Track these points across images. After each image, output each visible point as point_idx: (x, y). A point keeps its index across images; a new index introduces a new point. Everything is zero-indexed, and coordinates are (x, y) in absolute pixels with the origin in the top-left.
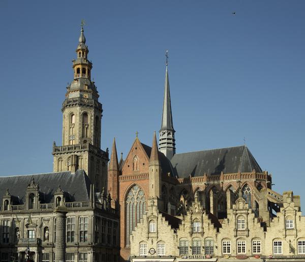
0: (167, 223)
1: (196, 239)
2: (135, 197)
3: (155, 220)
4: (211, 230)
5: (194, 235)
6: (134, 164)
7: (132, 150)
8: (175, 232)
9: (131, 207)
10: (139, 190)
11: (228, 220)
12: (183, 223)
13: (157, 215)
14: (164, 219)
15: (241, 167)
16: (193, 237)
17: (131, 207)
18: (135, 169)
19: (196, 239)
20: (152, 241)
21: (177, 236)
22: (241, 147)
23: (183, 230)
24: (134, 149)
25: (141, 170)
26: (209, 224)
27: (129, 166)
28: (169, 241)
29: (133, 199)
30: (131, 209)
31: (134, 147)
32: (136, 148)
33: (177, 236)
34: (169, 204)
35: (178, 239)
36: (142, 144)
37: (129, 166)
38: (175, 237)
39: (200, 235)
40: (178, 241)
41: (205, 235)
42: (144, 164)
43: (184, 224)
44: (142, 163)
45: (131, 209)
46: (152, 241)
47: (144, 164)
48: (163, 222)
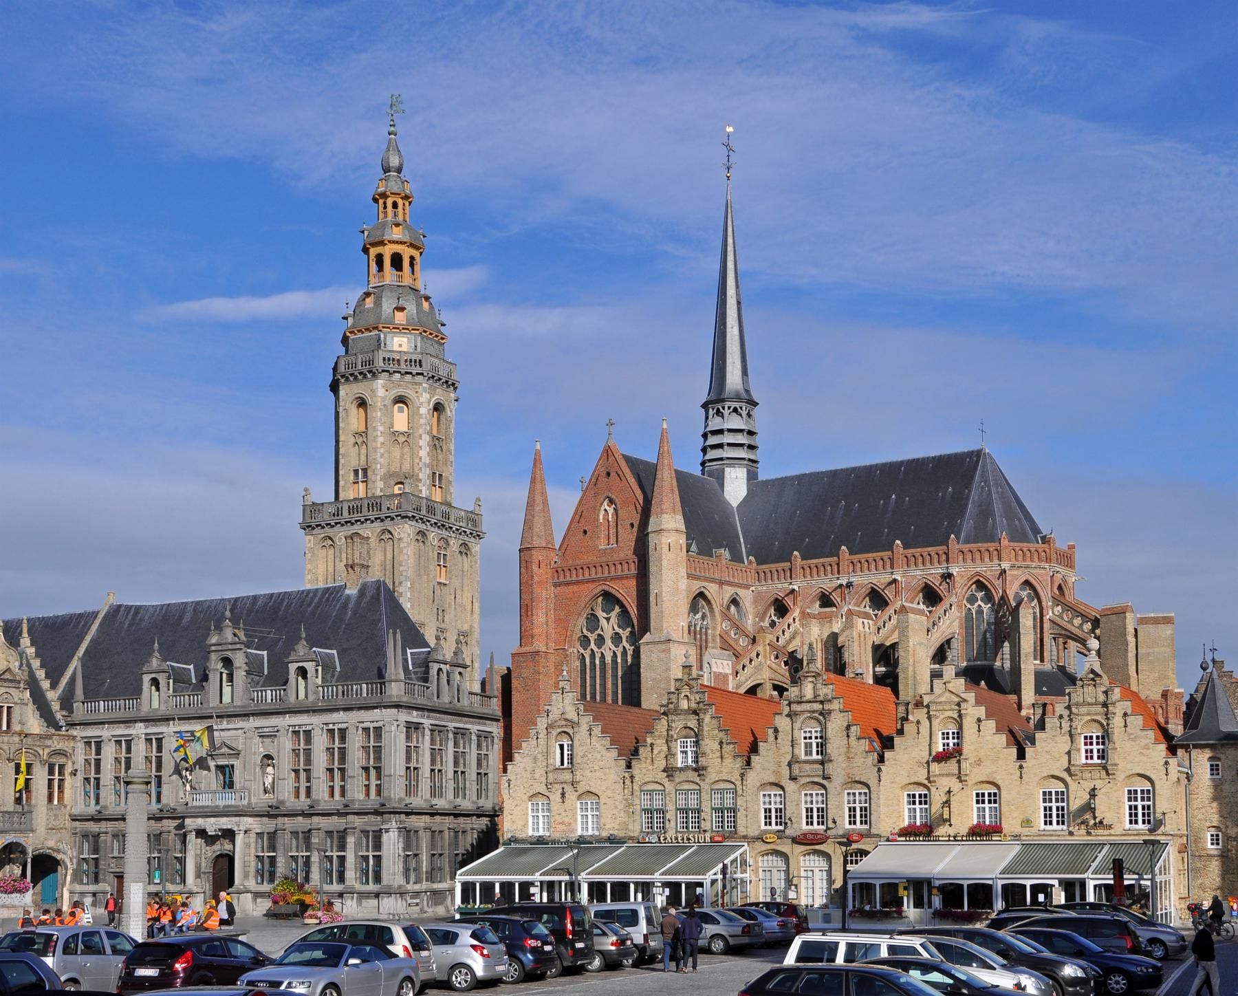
0: (607, 742)
1: (686, 786)
4: (728, 761)
5: (679, 777)
8: (629, 766)
11: (776, 730)
12: (649, 740)
13: (576, 719)
14: (597, 730)
15: (968, 524)
16: (677, 780)
19: (686, 786)
20: (563, 795)
21: (632, 777)
22: (970, 454)
23: (649, 761)
24: (603, 479)
26: (721, 743)
27: (585, 532)
28: (609, 793)
33: (632, 777)
35: (636, 787)
38: (628, 782)
39: (693, 776)
40: (637, 793)
41: (712, 775)
43: (652, 745)
46: (563, 795)
48: (594, 739)
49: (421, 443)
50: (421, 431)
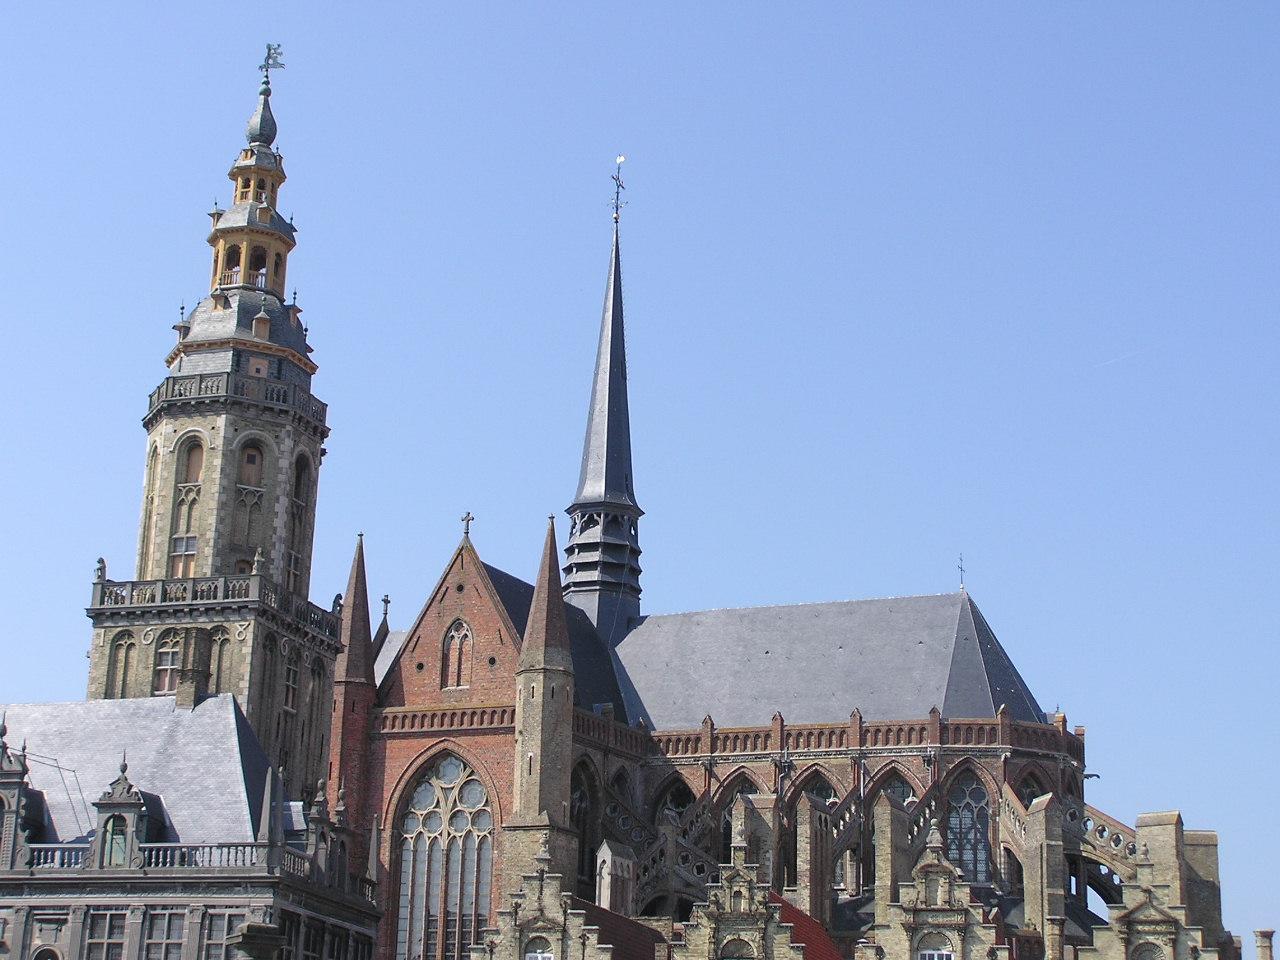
2: (444, 813)
3: (553, 938)
6: (445, 659)
7: (439, 595)
9: (423, 857)
10: (462, 777)
13: (561, 919)
14: (593, 938)
17: (423, 857)
18: (452, 679)
24: (452, 592)
25: (472, 690)
27: (420, 666)
29: (433, 822)
30: (423, 867)
31: (452, 581)
32: (460, 588)
34: (605, 854)
36: (487, 567)
37: (420, 666)
42: (492, 661)
44: (489, 653)
45: (423, 867)
47: (492, 661)
49: (278, 508)
50: (279, 491)
